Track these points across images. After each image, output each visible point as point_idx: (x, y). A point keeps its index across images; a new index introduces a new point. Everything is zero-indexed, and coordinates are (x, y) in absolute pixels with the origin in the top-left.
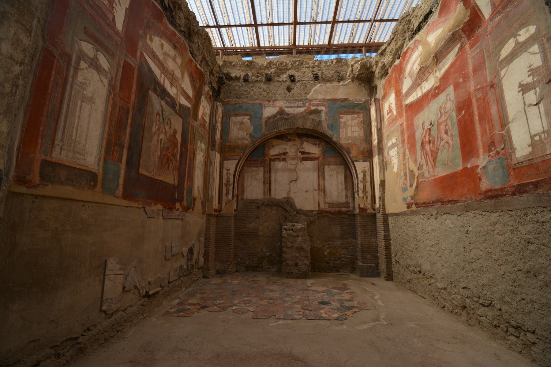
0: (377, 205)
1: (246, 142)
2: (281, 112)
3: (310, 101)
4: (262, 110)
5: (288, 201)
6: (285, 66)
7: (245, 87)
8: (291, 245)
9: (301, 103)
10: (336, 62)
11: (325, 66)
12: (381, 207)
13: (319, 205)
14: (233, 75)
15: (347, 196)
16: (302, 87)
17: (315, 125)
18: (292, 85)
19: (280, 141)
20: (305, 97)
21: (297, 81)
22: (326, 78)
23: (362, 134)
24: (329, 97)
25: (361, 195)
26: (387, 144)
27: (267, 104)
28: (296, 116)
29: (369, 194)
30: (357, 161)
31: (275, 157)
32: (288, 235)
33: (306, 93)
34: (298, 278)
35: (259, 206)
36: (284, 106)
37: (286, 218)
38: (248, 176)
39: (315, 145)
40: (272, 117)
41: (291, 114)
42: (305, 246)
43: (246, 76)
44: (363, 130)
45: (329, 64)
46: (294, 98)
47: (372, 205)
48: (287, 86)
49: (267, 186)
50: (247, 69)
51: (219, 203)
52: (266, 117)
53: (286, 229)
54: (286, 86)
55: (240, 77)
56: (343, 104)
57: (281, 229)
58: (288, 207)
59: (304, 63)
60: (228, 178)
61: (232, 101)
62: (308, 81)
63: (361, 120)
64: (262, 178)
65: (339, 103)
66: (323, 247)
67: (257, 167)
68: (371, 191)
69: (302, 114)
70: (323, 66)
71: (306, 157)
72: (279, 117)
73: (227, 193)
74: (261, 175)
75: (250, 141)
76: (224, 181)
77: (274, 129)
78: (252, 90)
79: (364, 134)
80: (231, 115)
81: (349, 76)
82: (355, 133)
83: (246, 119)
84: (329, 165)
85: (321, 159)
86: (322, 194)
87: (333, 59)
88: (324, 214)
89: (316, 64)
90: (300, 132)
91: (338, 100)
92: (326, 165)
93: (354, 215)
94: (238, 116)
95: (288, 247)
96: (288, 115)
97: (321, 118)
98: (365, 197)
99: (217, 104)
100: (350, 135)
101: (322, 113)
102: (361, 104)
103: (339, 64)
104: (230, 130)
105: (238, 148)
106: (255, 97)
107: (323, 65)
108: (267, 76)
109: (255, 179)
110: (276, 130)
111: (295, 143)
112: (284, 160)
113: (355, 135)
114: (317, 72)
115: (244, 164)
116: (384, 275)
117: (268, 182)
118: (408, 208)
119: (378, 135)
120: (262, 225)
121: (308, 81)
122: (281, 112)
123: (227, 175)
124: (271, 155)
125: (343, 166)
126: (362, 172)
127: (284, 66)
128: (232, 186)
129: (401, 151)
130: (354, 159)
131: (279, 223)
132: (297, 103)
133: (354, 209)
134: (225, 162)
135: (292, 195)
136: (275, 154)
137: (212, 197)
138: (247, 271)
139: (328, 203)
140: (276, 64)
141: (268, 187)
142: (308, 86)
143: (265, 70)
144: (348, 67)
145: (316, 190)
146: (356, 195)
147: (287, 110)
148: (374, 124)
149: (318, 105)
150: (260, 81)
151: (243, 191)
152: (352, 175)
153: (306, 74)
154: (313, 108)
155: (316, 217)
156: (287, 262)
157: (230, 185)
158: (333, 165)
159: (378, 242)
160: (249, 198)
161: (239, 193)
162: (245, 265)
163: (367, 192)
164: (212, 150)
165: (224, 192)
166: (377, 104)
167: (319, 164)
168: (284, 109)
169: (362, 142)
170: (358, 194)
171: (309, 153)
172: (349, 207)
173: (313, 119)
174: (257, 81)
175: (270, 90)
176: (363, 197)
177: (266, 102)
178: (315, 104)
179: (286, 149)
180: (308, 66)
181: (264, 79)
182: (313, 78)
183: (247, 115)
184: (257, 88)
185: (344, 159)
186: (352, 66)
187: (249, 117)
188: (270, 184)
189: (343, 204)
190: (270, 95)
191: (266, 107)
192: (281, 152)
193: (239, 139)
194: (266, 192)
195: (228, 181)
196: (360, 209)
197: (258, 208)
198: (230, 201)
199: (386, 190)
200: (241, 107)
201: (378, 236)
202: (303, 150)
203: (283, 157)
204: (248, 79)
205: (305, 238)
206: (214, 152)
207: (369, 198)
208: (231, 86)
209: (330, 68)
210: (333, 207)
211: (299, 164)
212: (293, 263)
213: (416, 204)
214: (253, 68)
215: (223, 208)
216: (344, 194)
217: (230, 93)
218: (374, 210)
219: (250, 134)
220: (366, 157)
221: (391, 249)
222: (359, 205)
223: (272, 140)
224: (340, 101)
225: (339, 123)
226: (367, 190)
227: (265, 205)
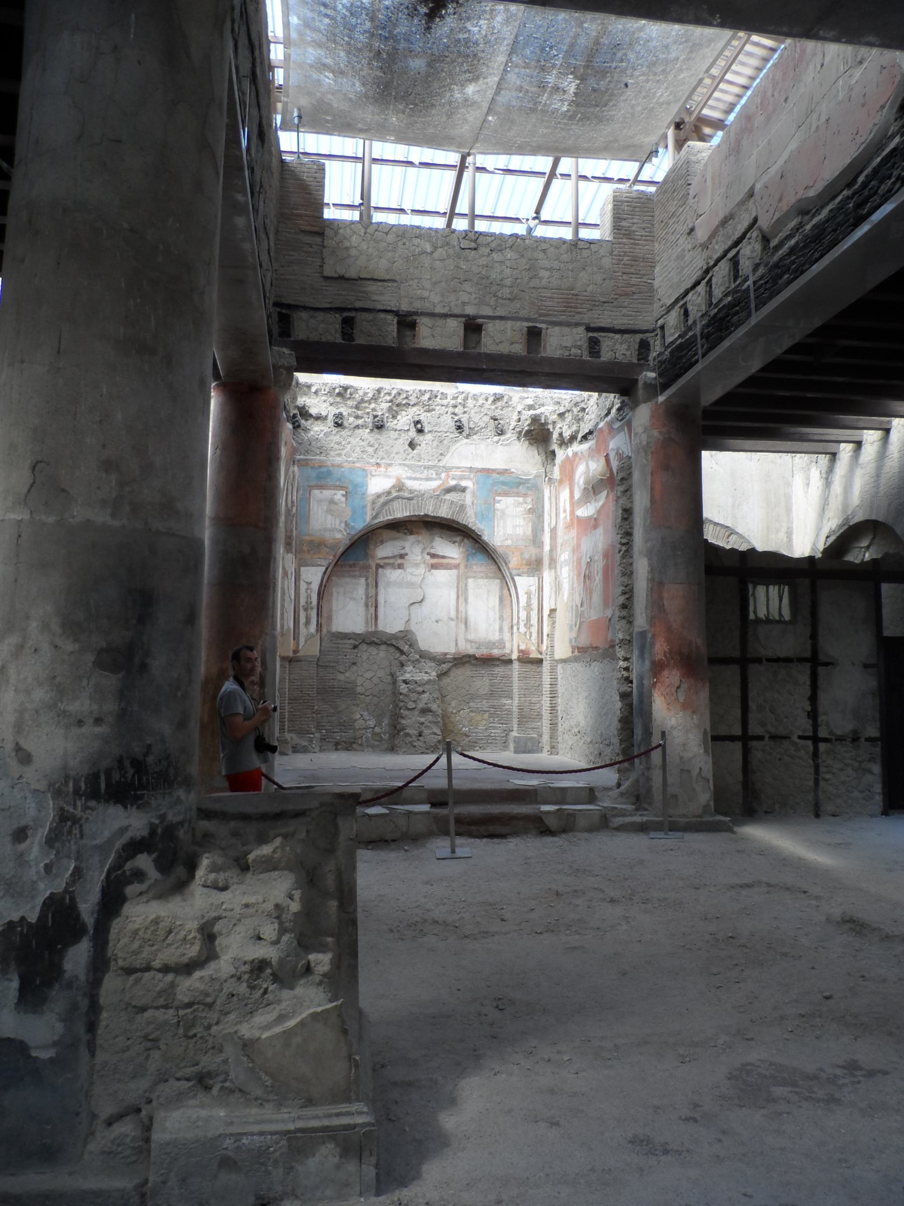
0: (544, 647)
1: (339, 536)
2: (400, 487)
3: (447, 469)
4: (367, 481)
5: (406, 636)
6: (407, 398)
7: (335, 435)
8: (414, 706)
9: (434, 472)
10: (494, 401)
11: (475, 406)
12: (549, 650)
13: (457, 644)
14: (313, 411)
15: (501, 630)
16: (435, 443)
17: (454, 512)
18: (419, 439)
19: (393, 533)
20: (439, 461)
21: (426, 431)
22: (476, 429)
23: (529, 531)
24: (479, 465)
25: (523, 629)
26: (560, 556)
27: (375, 471)
28: (424, 495)
29: (534, 630)
30: (519, 575)
31: (387, 561)
32: (410, 690)
33: (441, 454)
34: (422, 753)
35: (357, 643)
36: (404, 476)
37: (402, 665)
38: (338, 593)
39: (454, 542)
40: (383, 493)
41: (416, 491)
42: (434, 707)
43: (339, 416)
44: (530, 524)
45: (481, 401)
46: (420, 463)
47: (538, 646)
48: (410, 440)
49: (372, 610)
50: (338, 399)
51: (294, 639)
52: (373, 492)
53: (405, 682)
54: (407, 439)
55: (326, 416)
56: (502, 478)
57: (395, 682)
58: (407, 647)
59: (439, 397)
60: (309, 597)
61: (313, 462)
62: (446, 432)
63: (529, 507)
64: (364, 597)
65: (495, 475)
66: (461, 712)
67: (354, 577)
68: (538, 625)
69: (434, 492)
70: (472, 406)
71: (437, 563)
72: (395, 494)
73: (308, 622)
74: (360, 591)
75: (345, 534)
76: (303, 602)
77: (387, 515)
78: (349, 443)
79: (532, 531)
80: (311, 488)
81: (514, 429)
82: (518, 528)
83: (339, 495)
84: (474, 577)
85: (462, 567)
86: (463, 626)
87: (489, 394)
88: (465, 660)
89: (459, 400)
90: (430, 520)
91: (494, 471)
92: (470, 577)
93: (510, 661)
94: (324, 489)
95: (409, 709)
96: (411, 491)
97: (464, 501)
98: (528, 633)
99: (293, 472)
100: (510, 531)
101: (467, 491)
102: (529, 479)
103: (499, 404)
104: (311, 512)
105: (326, 546)
106: (354, 455)
107: (470, 404)
108: (376, 419)
109: (350, 599)
110: (390, 518)
111: (420, 538)
112: (400, 566)
113: (518, 533)
114: (462, 416)
115: (332, 571)
116: (547, 748)
117: (374, 605)
118: (573, 652)
119: (551, 538)
120: (362, 676)
121: (446, 432)
122: (400, 487)
123: (306, 592)
124: (379, 557)
125: (498, 581)
126: (526, 593)
127: (403, 399)
128: (315, 611)
129: (571, 574)
130: (514, 572)
131: (391, 673)
132: (425, 472)
133: (512, 652)
134: (302, 569)
135: (413, 627)
136: (386, 556)
137: (289, 629)
138: (337, 749)
139: (472, 642)
140: (389, 394)
141: (373, 612)
142: (445, 442)
143: (370, 403)
144: (512, 411)
145: (452, 620)
146: (515, 628)
147: (410, 484)
148: (546, 517)
149: (462, 478)
150: (364, 426)
151: (330, 618)
152: (511, 596)
153: (442, 419)
154: (453, 483)
155: (451, 664)
156: (407, 731)
157: (312, 609)
158: (482, 578)
159: (543, 702)
160: (341, 629)
161: (323, 622)
162: (334, 740)
163: (532, 625)
164: (288, 552)
165: (302, 620)
166: (552, 488)
167: (458, 576)
168: (403, 481)
169: (527, 544)
170: (518, 629)
171: (444, 557)
172: (504, 647)
173: (452, 502)
174: (357, 427)
175: (379, 444)
176: (526, 633)
177: (373, 466)
178: (456, 475)
179: (404, 548)
180: (445, 402)
181: (370, 420)
182: (454, 428)
183: (341, 488)
184: (357, 439)
185: (500, 569)
186: (519, 412)
187: (344, 493)
188: (376, 607)
189: (494, 644)
190: (381, 453)
191: (373, 476)
192: (397, 552)
193: (325, 530)
194: (370, 620)
195: (308, 603)
196: (520, 651)
197: (355, 647)
198: (312, 636)
199: (557, 625)
200: (329, 473)
201: (544, 693)
202: (432, 551)
203: (399, 561)
204: (342, 423)
205: (435, 695)
206: (290, 555)
207: (535, 635)
208: (312, 433)
209: (483, 410)
210: (478, 648)
211: (426, 574)
212: (416, 732)
213: (578, 648)
214: (349, 398)
215: (300, 648)
216: (497, 626)
217: (310, 445)
218: (541, 653)
219: (346, 522)
220: (533, 568)
221: (557, 711)
222: (518, 647)
223: (381, 531)
224: (498, 473)
225: (494, 511)
226: (532, 623)
227: (367, 643)
